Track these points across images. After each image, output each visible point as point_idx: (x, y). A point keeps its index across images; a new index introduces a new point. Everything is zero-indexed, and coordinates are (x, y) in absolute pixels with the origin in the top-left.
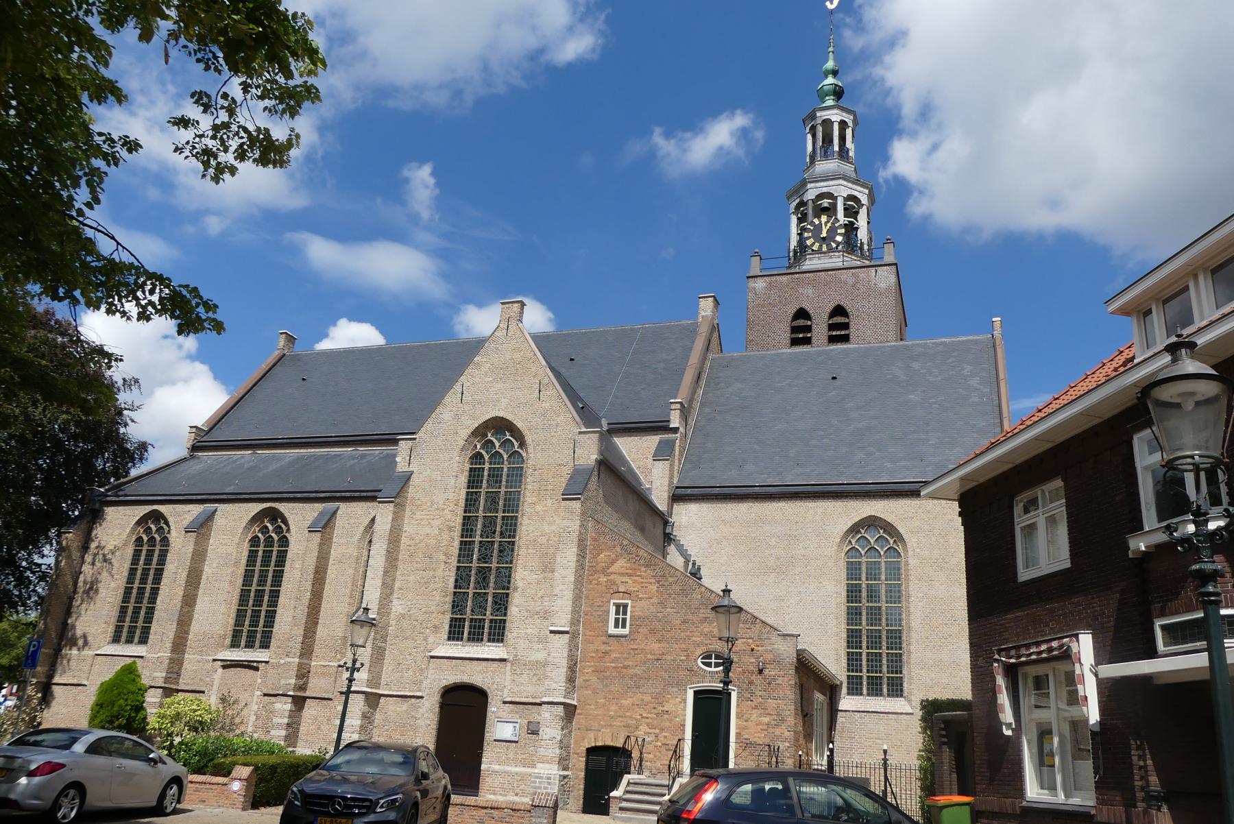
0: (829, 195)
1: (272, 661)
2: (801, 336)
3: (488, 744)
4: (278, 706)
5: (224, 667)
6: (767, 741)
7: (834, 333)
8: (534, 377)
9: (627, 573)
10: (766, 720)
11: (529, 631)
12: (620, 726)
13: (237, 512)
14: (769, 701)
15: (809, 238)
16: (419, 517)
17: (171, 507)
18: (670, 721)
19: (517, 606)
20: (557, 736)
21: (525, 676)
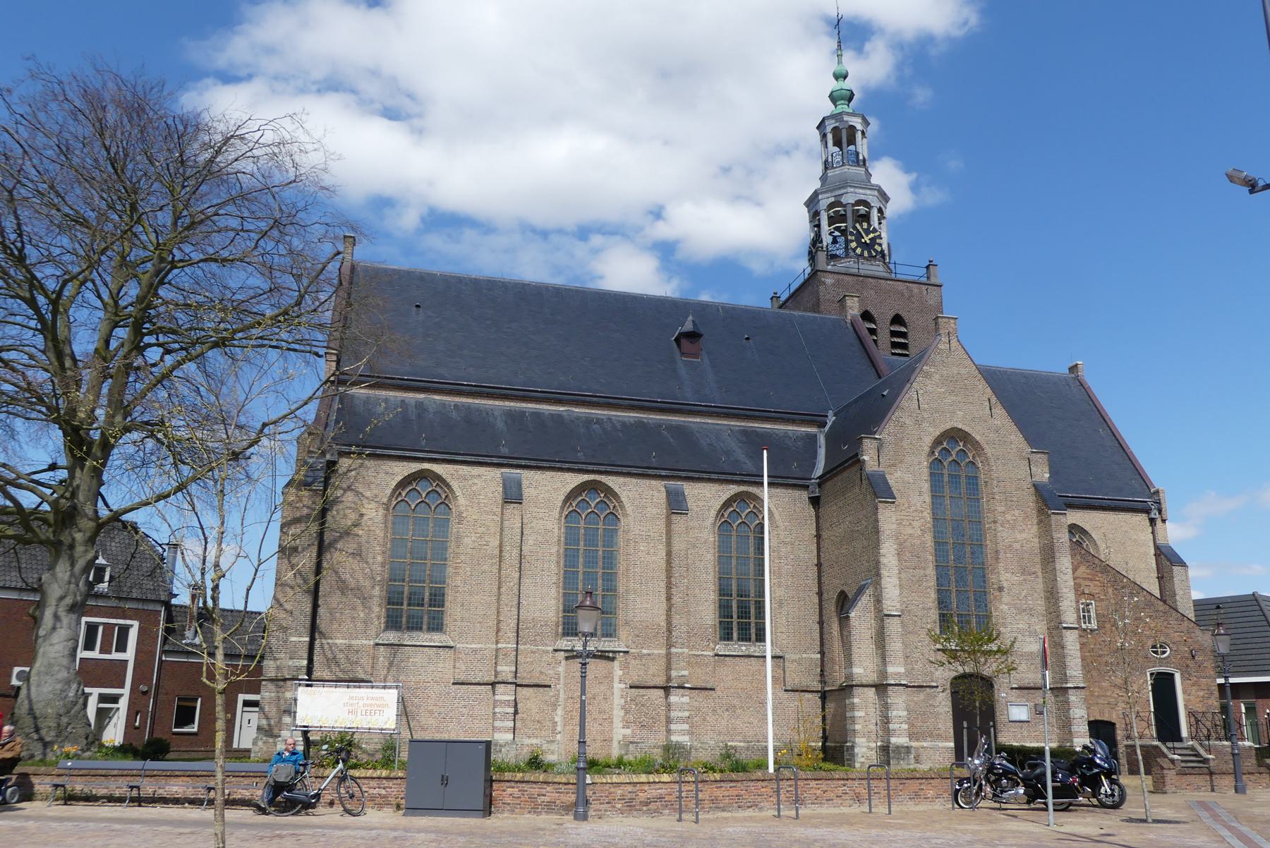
1: (632, 651)
5: (567, 658)
11: (1020, 626)
12: (1103, 704)
17: (450, 467)
19: (1006, 604)
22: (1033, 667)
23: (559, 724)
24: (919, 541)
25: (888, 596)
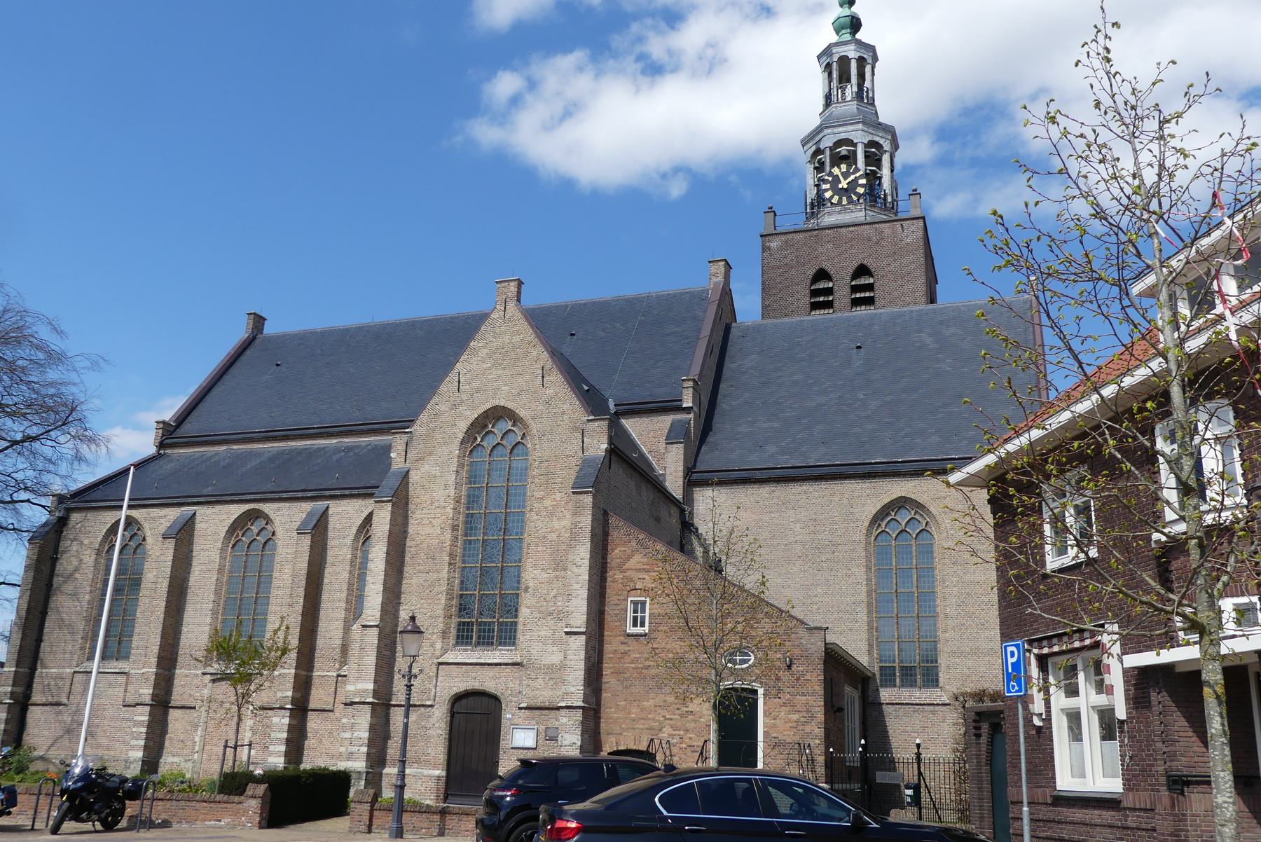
0: (849, 142)
2: (821, 299)
3: (505, 752)
4: (276, 720)
5: (214, 681)
6: (796, 739)
7: (858, 295)
8: (536, 362)
9: (644, 569)
10: (795, 717)
11: (542, 633)
12: (642, 729)
13: (218, 515)
14: (798, 697)
15: (827, 190)
16: (418, 516)
17: (144, 511)
18: (695, 721)
19: (528, 607)
20: (576, 742)
21: (541, 681)
22: (551, 682)
23: (198, 744)
24: (437, 541)
25: (369, 605)
